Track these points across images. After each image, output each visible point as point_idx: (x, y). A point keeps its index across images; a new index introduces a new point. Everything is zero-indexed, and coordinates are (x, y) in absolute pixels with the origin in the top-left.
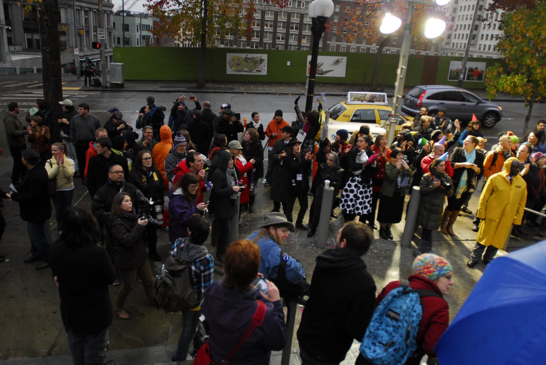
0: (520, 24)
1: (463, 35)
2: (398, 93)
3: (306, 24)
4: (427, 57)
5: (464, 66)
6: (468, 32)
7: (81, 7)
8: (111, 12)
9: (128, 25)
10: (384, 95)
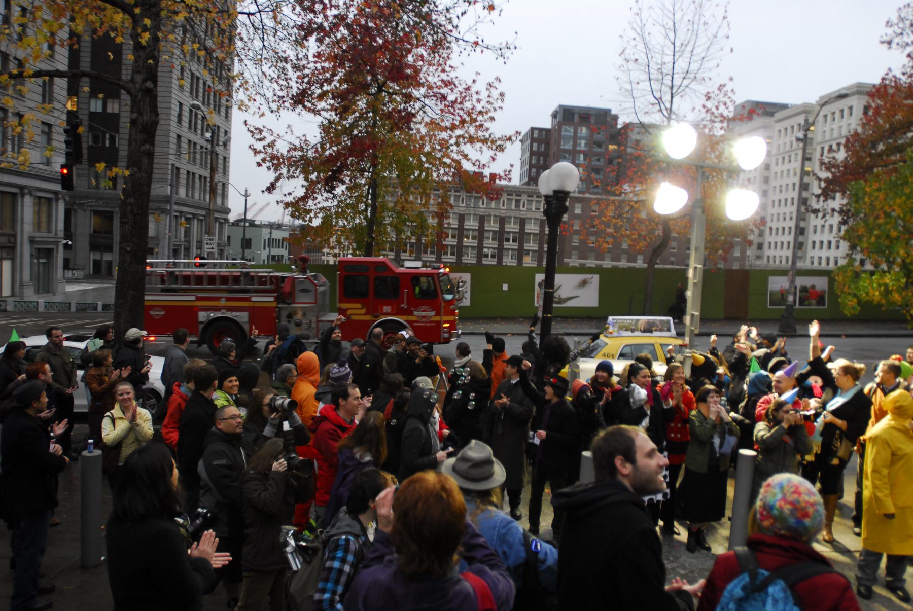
2: (693, 309)
3: (529, 234)
4: (730, 272)
5: (792, 282)
6: (791, 238)
7: (181, 212)
8: (227, 220)
9: (250, 240)
10: (669, 321)
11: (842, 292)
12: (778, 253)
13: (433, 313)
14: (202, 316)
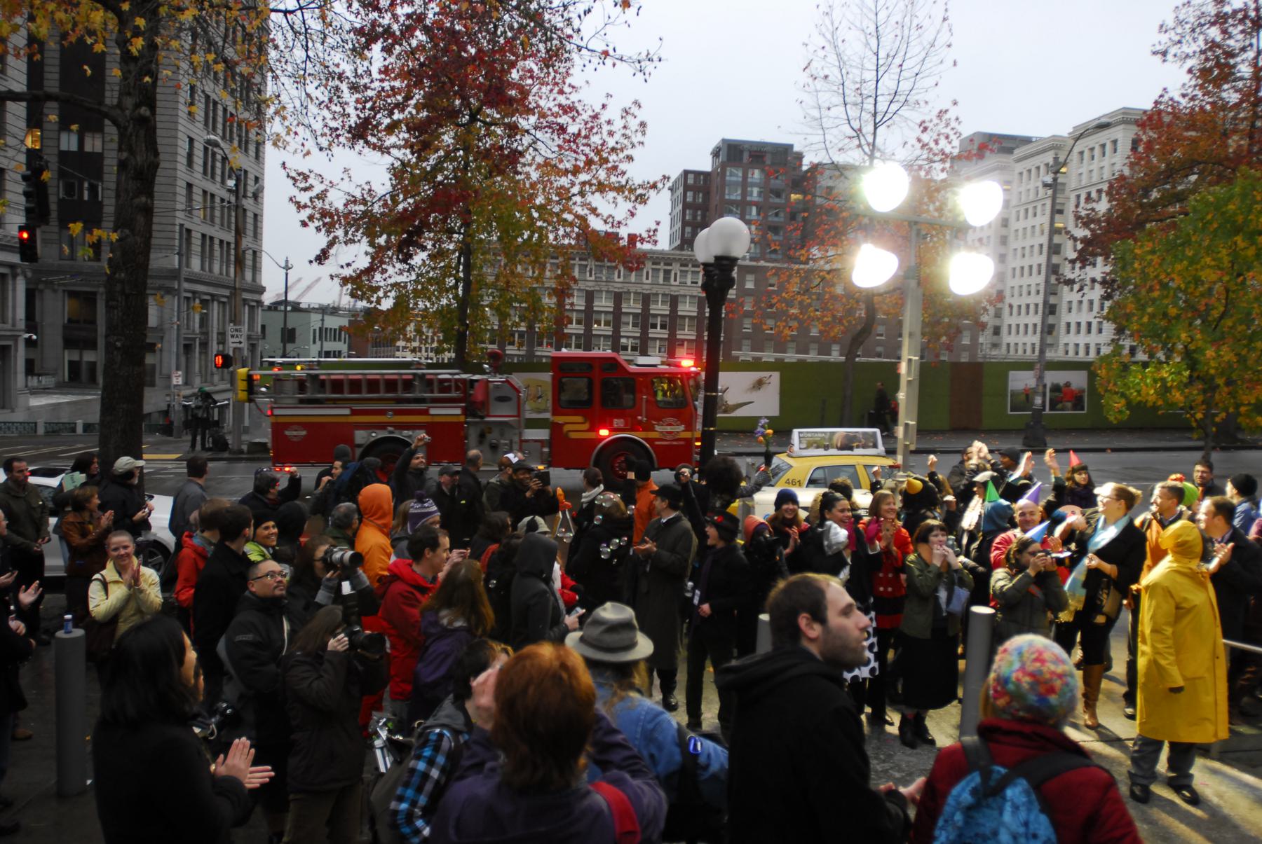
0: (1152, 260)
1: (1026, 326)
2: (907, 416)
3: (684, 317)
4: (956, 366)
5: (1040, 378)
6: (1038, 319)
7: (194, 292)
8: (260, 303)
9: (293, 330)
10: (875, 433)
11: (1106, 391)
12: (1021, 339)
13: (682, 428)
14: (361, 437)
